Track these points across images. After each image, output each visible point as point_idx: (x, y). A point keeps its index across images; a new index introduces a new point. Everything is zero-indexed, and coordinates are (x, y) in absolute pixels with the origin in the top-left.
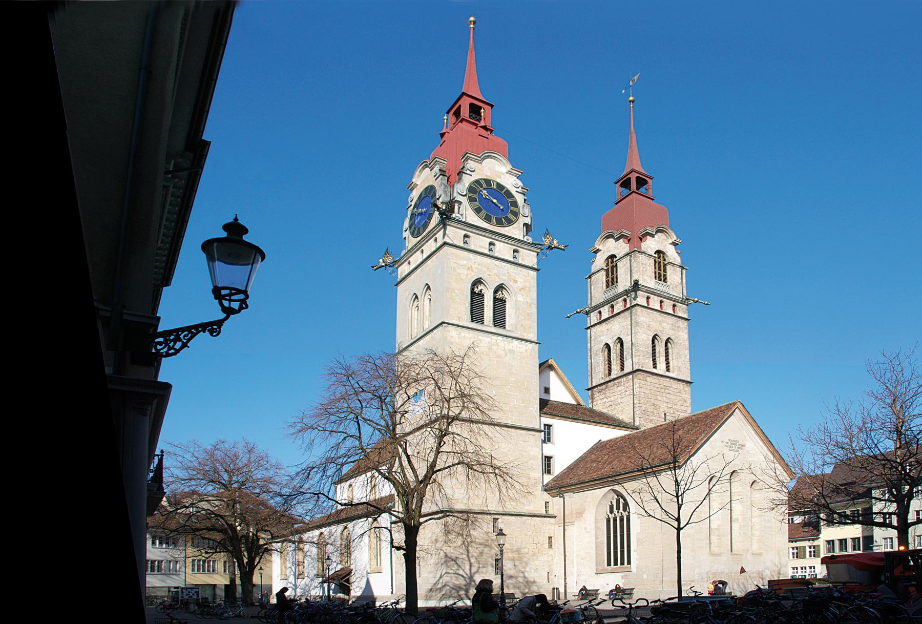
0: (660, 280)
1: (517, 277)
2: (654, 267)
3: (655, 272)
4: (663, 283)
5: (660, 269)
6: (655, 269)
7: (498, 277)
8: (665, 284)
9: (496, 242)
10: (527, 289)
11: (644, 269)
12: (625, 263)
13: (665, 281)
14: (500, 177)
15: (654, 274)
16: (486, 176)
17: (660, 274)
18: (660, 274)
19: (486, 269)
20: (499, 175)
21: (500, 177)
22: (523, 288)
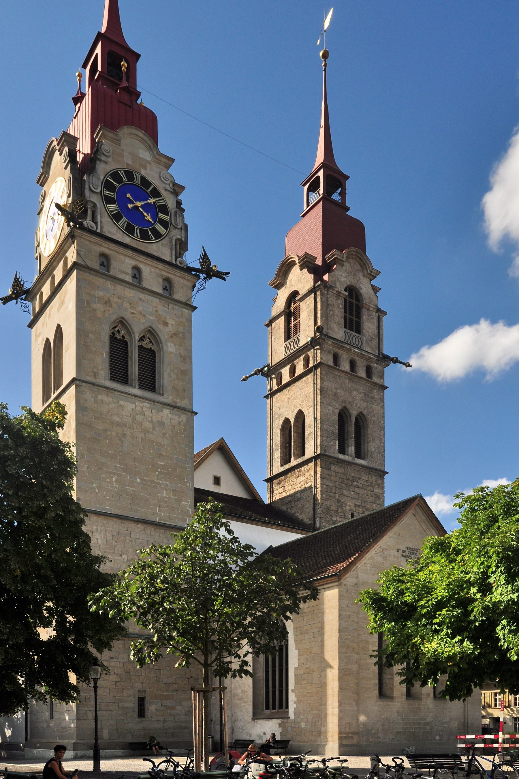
1: (168, 318)
2: (343, 310)
3: (345, 318)
4: (354, 334)
5: (351, 314)
6: (345, 312)
7: (144, 316)
8: (357, 335)
9: (141, 266)
10: (181, 335)
11: (331, 313)
12: (308, 303)
13: (358, 330)
15: (343, 320)
16: (127, 164)
17: (351, 320)
19: (128, 305)
20: (144, 164)
21: (145, 168)
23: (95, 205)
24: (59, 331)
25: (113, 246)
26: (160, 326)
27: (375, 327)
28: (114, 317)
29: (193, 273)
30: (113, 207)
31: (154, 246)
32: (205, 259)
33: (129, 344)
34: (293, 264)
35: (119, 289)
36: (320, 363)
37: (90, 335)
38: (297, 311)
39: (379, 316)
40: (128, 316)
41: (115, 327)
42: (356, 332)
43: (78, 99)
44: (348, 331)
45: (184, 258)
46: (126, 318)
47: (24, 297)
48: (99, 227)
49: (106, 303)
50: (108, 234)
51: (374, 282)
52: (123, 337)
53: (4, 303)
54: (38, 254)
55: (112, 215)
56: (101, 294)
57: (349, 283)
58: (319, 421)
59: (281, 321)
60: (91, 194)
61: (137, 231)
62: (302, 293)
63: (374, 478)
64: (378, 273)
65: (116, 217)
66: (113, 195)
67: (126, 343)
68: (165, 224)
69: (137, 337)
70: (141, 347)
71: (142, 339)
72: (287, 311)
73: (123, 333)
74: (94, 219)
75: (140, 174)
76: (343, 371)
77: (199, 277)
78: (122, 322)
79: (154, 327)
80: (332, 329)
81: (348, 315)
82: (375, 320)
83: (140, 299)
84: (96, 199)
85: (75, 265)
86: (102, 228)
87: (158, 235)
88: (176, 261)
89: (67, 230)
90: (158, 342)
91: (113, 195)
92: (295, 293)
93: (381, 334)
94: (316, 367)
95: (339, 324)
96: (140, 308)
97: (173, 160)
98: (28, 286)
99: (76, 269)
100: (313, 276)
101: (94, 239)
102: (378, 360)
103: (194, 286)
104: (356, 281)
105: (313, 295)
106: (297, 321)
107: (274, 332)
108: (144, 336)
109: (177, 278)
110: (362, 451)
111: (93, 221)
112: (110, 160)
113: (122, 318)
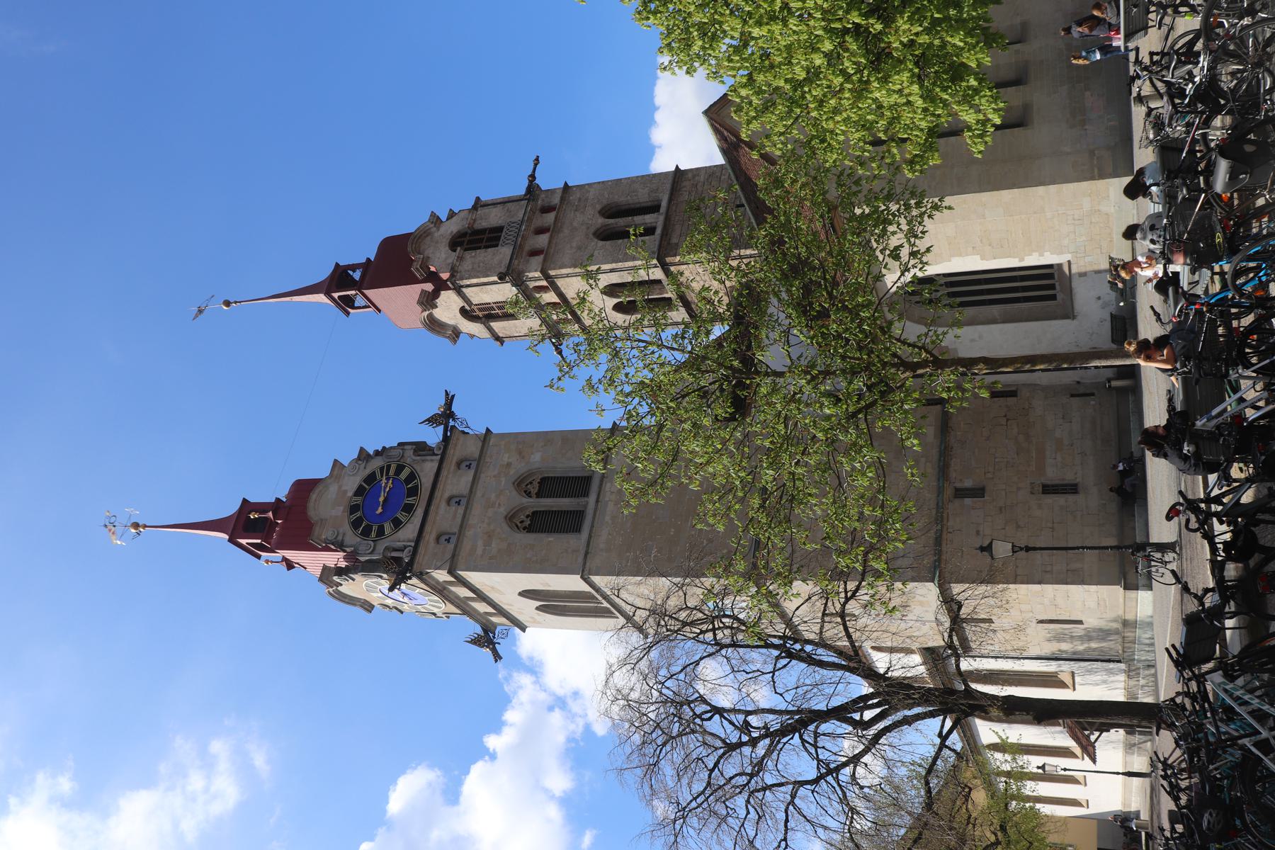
0: (498, 238)
2: (478, 251)
3: (487, 247)
4: (504, 234)
5: (481, 241)
6: (480, 248)
8: (505, 230)
9: (446, 495)
11: (481, 264)
12: (472, 294)
13: (499, 229)
14: (345, 492)
16: (344, 512)
17: (489, 239)
18: (489, 239)
21: (345, 492)
22: (520, 453)
23: (387, 548)
24: (527, 594)
25: (428, 528)
26: (512, 472)
27: (494, 210)
28: (506, 528)
29: (449, 434)
30: (388, 527)
31: (423, 480)
32: (432, 421)
33: (535, 509)
34: (431, 317)
35: (473, 520)
36: (541, 272)
37: (528, 556)
38: (485, 307)
39: (481, 206)
40: (503, 511)
41: (517, 526)
42: (502, 232)
43: (290, 565)
44: (501, 242)
45: (433, 446)
46: (505, 513)
47: (491, 635)
48: (409, 544)
49: (489, 536)
50: (415, 534)
51: (444, 219)
52: (528, 516)
53: (501, 658)
54: (444, 616)
55: (396, 528)
56: (480, 543)
57: (447, 248)
58: (614, 266)
59: (495, 325)
60: (376, 552)
61: (410, 500)
62: (461, 303)
63: (684, 184)
64: (433, 214)
65: (397, 524)
66: (375, 528)
67: (535, 513)
68: (400, 469)
69: (526, 501)
70: (539, 495)
71: (529, 494)
72: (483, 319)
74: (401, 550)
75: (351, 498)
76: (550, 242)
77: (453, 427)
78: (510, 518)
79: (513, 480)
80: (500, 262)
81: (484, 244)
82: (486, 210)
83: (483, 496)
84: (381, 546)
85: (450, 572)
86: (409, 541)
87: (412, 476)
88: (437, 455)
89: (414, 581)
90: (531, 474)
91: (375, 528)
92: (463, 312)
93: (502, 200)
94: (547, 277)
95: (494, 254)
96: (493, 496)
97: (336, 461)
98: (479, 630)
99: (455, 570)
100: (442, 292)
101: (421, 550)
102: (533, 200)
103: (463, 432)
104: (444, 240)
105: (464, 290)
106: (494, 305)
107: (509, 334)
108: (525, 492)
109: (455, 453)
110: (649, 204)
111: (403, 551)
112: (341, 531)
113: (506, 517)
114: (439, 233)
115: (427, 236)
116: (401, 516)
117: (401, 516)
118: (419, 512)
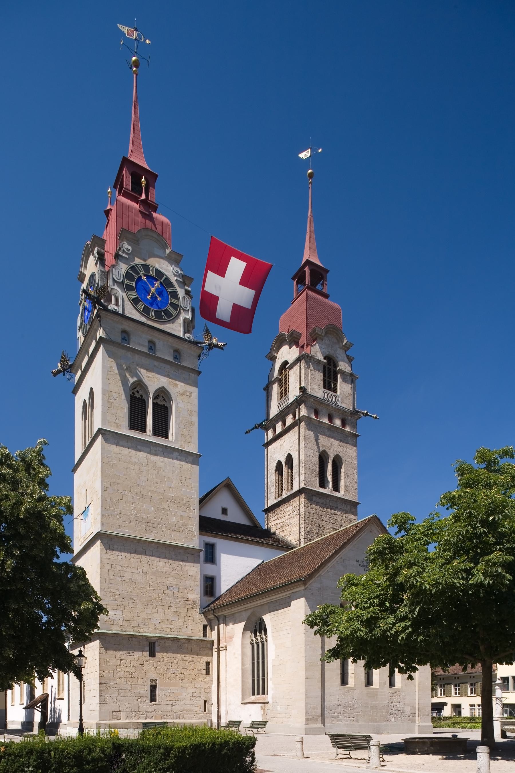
9: (156, 340)
12: (295, 370)
38: (287, 377)
41: (135, 388)
51: (348, 353)
52: (142, 396)
57: (327, 353)
65: (135, 302)
67: (144, 400)
73: (141, 393)
108: (158, 396)
114: (338, 349)
115: (337, 340)
116: (141, 306)
117: (141, 306)
118: (143, 320)
